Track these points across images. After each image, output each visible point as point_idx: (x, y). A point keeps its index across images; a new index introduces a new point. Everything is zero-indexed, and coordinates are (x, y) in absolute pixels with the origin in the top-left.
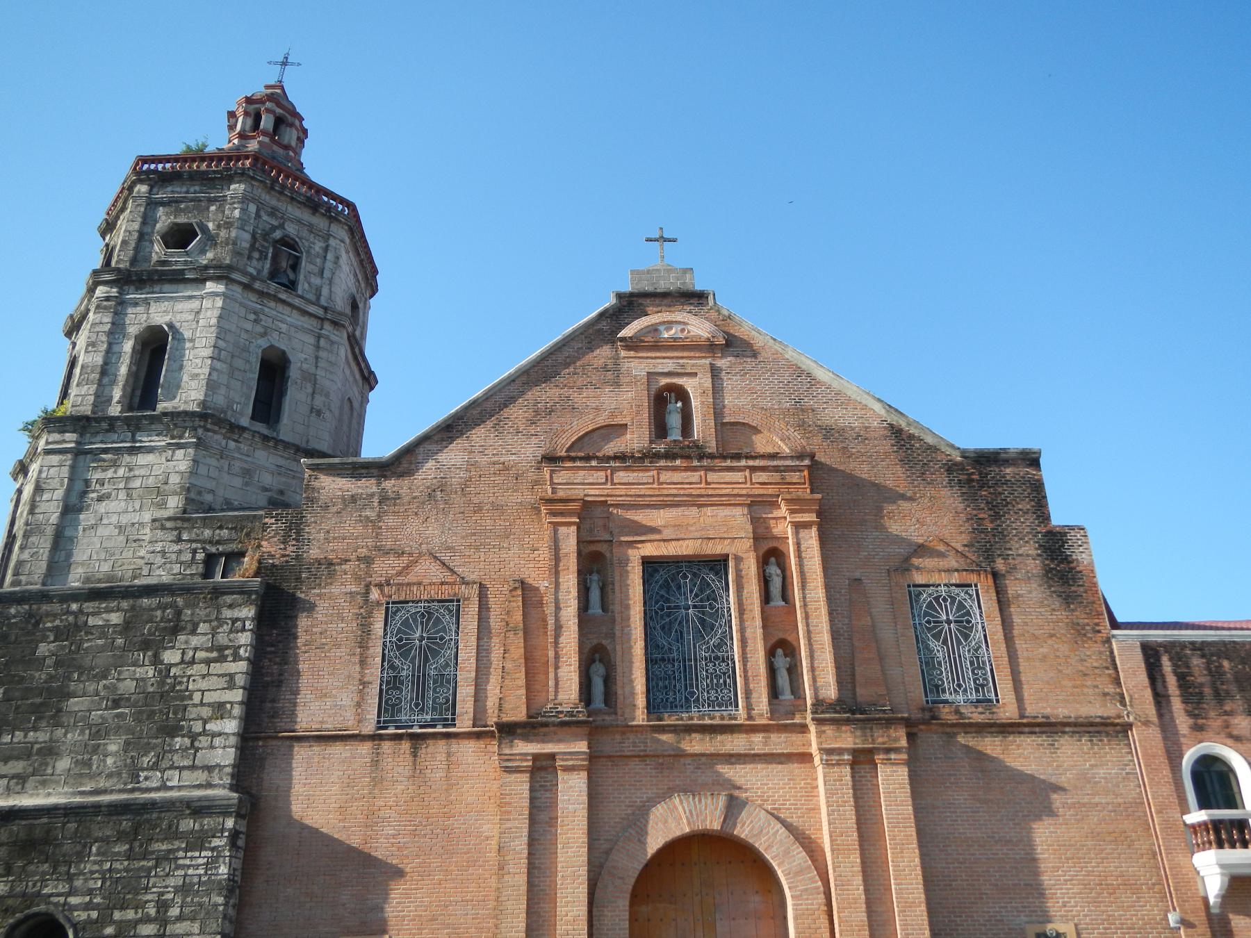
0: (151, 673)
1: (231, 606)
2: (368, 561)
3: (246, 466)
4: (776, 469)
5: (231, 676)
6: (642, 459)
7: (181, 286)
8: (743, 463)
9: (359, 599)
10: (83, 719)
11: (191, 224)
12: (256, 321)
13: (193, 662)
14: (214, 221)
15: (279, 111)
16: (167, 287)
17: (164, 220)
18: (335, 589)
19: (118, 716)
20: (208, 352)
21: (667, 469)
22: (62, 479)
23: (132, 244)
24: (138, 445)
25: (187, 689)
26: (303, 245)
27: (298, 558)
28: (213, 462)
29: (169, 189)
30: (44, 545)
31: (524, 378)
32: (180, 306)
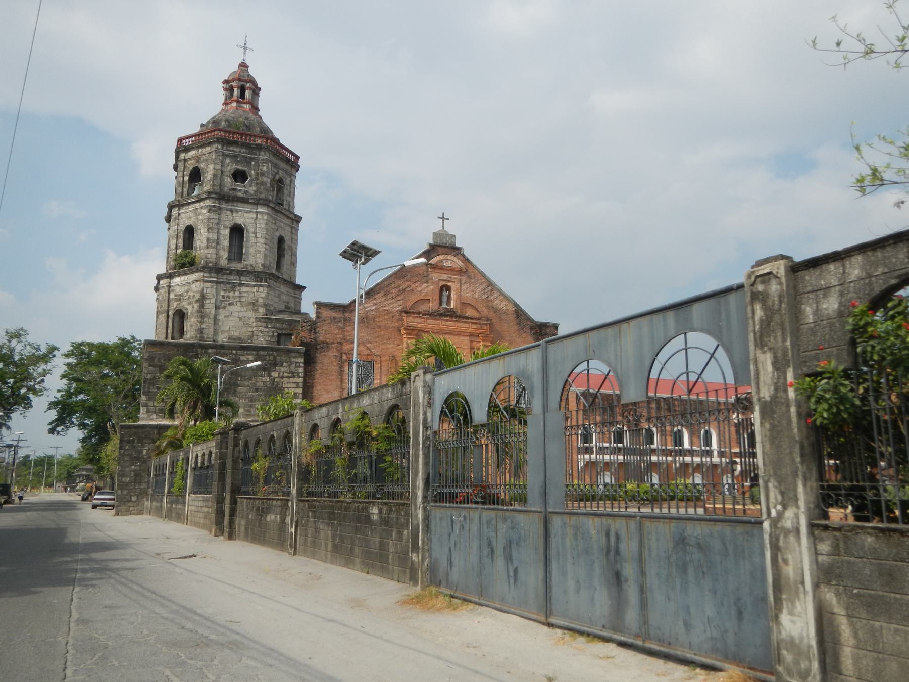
0: (268, 380)
1: (294, 357)
2: (340, 343)
3: (279, 293)
4: (480, 324)
5: (298, 383)
6: (436, 316)
7: (246, 205)
8: (469, 321)
9: (339, 358)
10: (246, 395)
11: (245, 171)
12: (275, 224)
13: (283, 377)
14: (254, 170)
15: (253, 87)
16: (239, 204)
17: (231, 166)
18: (330, 354)
19: (258, 395)
20: (262, 241)
21: (444, 320)
22: (213, 295)
23: (219, 177)
24: (243, 282)
25: (282, 387)
26: (284, 180)
27: (315, 340)
28: (272, 293)
29: (231, 148)
30: (209, 322)
31: (395, 276)
32: (247, 215)
